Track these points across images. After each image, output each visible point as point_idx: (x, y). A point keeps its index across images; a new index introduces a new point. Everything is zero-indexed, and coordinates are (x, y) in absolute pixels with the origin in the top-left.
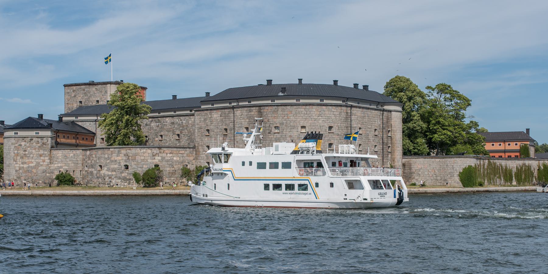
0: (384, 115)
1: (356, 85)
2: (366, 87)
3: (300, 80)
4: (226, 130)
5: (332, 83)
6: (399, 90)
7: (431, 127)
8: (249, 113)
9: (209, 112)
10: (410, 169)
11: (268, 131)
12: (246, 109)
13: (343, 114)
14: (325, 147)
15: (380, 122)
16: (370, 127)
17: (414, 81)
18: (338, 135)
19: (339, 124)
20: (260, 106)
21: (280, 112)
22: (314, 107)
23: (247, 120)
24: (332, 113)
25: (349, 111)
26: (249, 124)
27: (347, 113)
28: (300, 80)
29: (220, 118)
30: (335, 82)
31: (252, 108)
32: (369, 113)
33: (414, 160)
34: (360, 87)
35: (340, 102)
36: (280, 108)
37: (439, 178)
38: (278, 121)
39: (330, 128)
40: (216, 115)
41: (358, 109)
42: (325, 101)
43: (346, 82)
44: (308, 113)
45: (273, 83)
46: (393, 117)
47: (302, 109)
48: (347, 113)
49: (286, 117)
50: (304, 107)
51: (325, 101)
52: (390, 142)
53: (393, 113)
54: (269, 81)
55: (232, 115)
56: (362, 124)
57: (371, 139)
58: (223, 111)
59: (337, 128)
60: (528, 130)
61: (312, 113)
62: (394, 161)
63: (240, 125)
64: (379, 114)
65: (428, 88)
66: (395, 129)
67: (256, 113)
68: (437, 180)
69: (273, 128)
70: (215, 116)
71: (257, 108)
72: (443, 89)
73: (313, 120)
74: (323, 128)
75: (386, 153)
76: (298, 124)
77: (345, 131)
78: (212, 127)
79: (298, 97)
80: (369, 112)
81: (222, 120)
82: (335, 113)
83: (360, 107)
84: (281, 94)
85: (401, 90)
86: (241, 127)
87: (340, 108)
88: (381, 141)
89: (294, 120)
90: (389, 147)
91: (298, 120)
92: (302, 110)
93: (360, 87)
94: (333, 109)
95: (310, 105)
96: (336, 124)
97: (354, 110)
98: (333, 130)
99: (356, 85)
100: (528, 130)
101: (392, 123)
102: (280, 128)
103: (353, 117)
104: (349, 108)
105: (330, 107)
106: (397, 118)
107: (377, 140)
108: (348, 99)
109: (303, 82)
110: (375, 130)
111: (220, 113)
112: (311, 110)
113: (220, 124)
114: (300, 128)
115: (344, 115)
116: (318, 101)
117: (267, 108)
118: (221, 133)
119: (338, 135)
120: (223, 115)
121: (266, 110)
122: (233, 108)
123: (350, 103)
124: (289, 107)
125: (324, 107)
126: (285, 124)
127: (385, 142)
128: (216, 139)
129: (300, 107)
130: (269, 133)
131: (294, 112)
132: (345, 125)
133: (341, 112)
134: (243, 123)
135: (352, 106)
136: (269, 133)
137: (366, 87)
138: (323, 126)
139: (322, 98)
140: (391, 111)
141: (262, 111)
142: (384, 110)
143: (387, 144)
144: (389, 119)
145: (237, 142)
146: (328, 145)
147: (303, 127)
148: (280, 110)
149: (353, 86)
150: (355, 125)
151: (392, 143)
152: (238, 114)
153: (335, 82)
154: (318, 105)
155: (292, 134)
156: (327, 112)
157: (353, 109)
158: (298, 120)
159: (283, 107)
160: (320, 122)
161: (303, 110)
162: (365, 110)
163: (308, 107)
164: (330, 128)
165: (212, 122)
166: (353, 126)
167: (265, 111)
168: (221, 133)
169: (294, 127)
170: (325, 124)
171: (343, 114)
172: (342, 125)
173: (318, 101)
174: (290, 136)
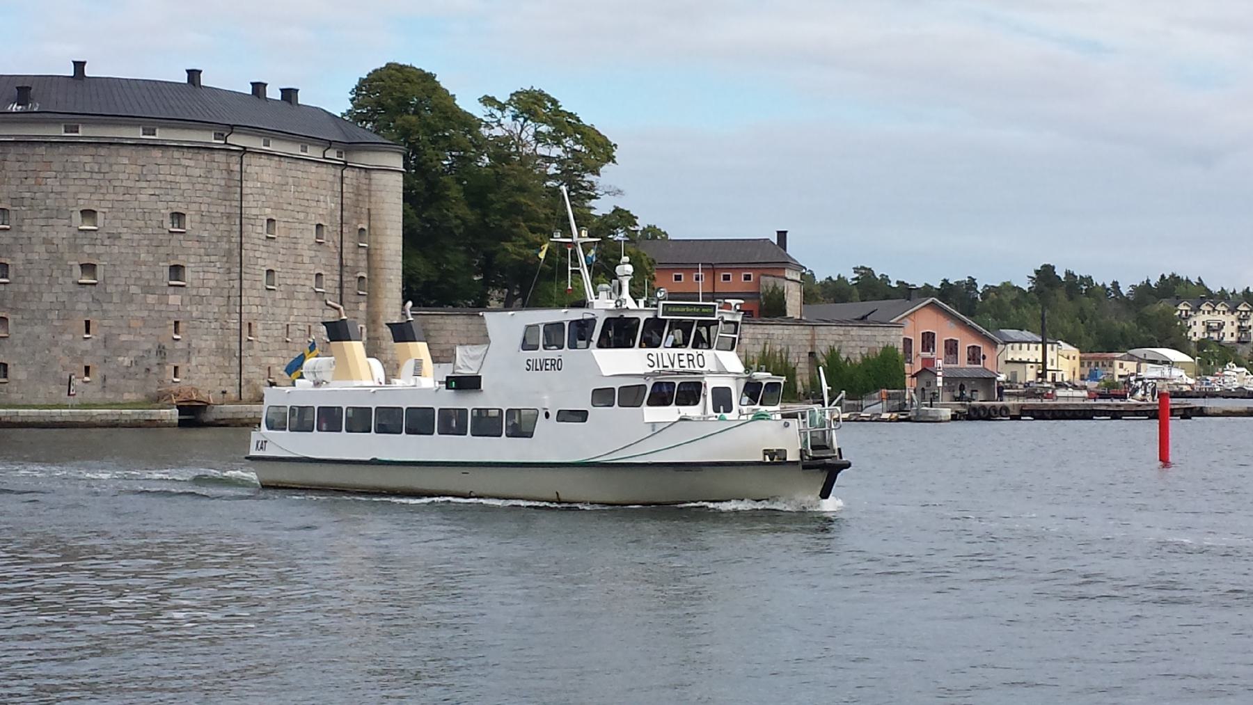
0: (346, 181)
1: (259, 88)
2: (289, 95)
3: (79, 66)
5: (184, 79)
6: (400, 104)
7: (494, 219)
13: (216, 174)
14: (159, 276)
15: (333, 205)
16: (301, 216)
17: (444, 81)
19: (204, 208)
22: (123, 151)
24: (181, 171)
25: (237, 168)
28: (79, 66)
30: (194, 75)
32: (300, 174)
33: (438, 320)
34: (273, 93)
35: (208, 138)
39: (178, 217)
41: (264, 160)
42: (160, 135)
43: (228, 75)
44: (105, 168)
46: (373, 188)
47: (84, 158)
48: (230, 172)
49: (31, 181)
50: (92, 150)
51: (160, 135)
52: (363, 264)
53: (376, 176)
56: (275, 208)
57: (307, 254)
59: (197, 218)
60: (782, 235)
61: (115, 168)
62: (374, 322)
64: (331, 178)
65: (488, 101)
72: (531, 104)
73: (121, 190)
74: (153, 216)
75: (353, 299)
76: (71, 201)
77: (222, 227)
79: (73, 119)
80: (298, 171)
82: (189, 171)
83: (270, 155)
84: (15, 108)
85: (403, 105)
87: (206, 156)
88: (337, 262)
89: (59, 189)
90: (362, 278)
91: (72, 189)
93: (273, 93)
94: (187, 160)
96: (195, 207)
97: (254, 166)
99: (259, 88)
100: (782, 235)
101: (372, 207)
102: (13, 215)
103: (248, 186)
104: (236, 159)
105: (177, 154)
106: (389, 192)
107: (323, 257)
108: (232, 128)
109: (88, 72)
110: (319, 226)
112: (112, 160)
114: (77, 217)
115: (218, 177)
116: (138, 133)
119: (200, 239)
123: (237, 140)
124: (41, 150)
125: (157, 153)
126: (27, 202)
127: (350, 263)
129: (79, 149)
131: (55, 166)
132: (222, 209)
135: (245, 150)
137: (289, 95)
139: (150, 123)
143: (354, 271)
144: (364, 193)
146: (167, 270)
147: (88, 214)
150: (255, 212)
151: (369, 269)
153: (194, 75)
157: (246, 159)
158: (72, 189)
159: (23, 149)
160: (143, 197)
161: (88, 159)
162: (285, 164)
163: (103, 151)
166: (246, 212)
169: (57, 213)
170: (160, 205)
171: (216, 174)
172: (213, 209)
173: (138, 133)
174: (48, 242)
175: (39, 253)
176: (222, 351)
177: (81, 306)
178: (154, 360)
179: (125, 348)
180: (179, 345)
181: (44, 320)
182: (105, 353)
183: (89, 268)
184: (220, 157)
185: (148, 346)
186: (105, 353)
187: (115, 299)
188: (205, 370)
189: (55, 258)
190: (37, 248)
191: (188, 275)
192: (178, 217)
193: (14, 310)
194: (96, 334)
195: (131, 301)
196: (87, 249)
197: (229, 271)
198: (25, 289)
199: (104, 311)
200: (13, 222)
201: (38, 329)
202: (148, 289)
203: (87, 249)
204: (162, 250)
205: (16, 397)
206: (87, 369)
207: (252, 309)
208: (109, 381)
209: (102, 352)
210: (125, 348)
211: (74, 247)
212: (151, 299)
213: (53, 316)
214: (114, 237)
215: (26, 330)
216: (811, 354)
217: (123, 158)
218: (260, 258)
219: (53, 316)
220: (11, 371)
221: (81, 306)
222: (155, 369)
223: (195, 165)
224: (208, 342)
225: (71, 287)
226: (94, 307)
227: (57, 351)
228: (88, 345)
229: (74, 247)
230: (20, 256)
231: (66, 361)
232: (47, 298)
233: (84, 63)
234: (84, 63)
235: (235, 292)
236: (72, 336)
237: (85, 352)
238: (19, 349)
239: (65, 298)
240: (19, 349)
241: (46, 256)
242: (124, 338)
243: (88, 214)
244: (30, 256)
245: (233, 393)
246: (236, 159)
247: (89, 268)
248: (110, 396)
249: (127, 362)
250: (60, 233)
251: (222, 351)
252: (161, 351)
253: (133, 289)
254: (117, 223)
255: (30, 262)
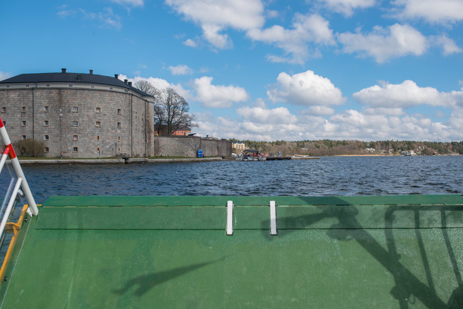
2: (130, 83)
3: (91, 71)
4: (24, 108)
8: (49, 95)
9: (5, 92)
10: (158, 144)
11: (67, 111)
12: (46, 91)
13: (127, 100)
18: (124, 116)
20: (60, 89)
21: (78, 95)
22: (107, 93)
23: (47, 100)
26: (49, 104)
27: (130, 100)
28: (91, 71)
29: (17, 98)
31: (52, 91)
36: (79, 92)
37: (178, 151)
38: (77, 102)
39: (119, 110)
40: (13, 95)
42: (114, 89)
45: (67, 71)
47: (97, 94)
48: (130, 100)
50: (99, 92)
51: (114, 89)
53: (150, 104)
54: (64, 70)
55: (31, 95)
58: (21, 91)
61: (105, 97)
63: (39, 105)
66: (151, 115)
67: (57, 95)
68: (177, 153)
69: (72, 108)
70: (12, 96)
71: (57, 91)
76: (94, 106)
78: (9, 105)
81: (19, 100)
86: (41, 106)
89: (91, 102)
91: (94, 102)
92: (97, 94)
95: (104, 91)
98: (122, 112)
99: (126, 81)
105: (119, 94)
109: (94, 73)
111: (17, 93)
113: (18, 103)
114: (95, 109)
117: (66, 91)
118: (19, 111)
119: (124, 116)
120: (21, 95)
121: (65, 93)
122: (33, 89)
124: (86, 92)
125: (114, 94)
126: (83, 105)
128: (13, 116)
130: (69, 112)
131: (90, 96)
133: (126, 99)
134: (43, 103)
135: (133, 95)
136: (68, 112)
138: (114, 109)
140: (148, 102)
141: (62, 93)
142: (146, 101)
144: (148, 107)
145: (37, 119)
147: (98, 108)
148: (78, 93)
149: (124, 81)
152: (37, 95)
154: (110, 91)
155: (89, 114)
156: (116, 98)
157: (133, 97)
158: (94, 102)
159: (81, 91)
160: (112, 105)
161: (98, 95)
163: (102, 93)
164: (119, 110)
165: (8, 101)
167: (65, 93)
168: (19, 111)
169: (90, 108)
170: (115, 107)
171: (127, 100)
173: (108, 88)
174: (88, 116)
175: (86, 118)
176: (128, 145)
177: (97, 133)
178: (114, 147)
179: (108, 144)
180: (120, 143)
181: (87, 136)
182: (102, 145)
183: (98, 123)
184: (128, 96)
185: (113, 143)
186: (102, 145)
187: (105, 131)
188: (125, 149)
189: (90, 120)
190: (85, 117)
191: (122, 125)
192: (119, 110)
193: (79, 133)
194: (100, 140)
195: (109, 132)
196: (98, 118)
197: (129, 125)
198: (82, 128)
199: (102, 134)
200: (79, 110)
201: (86, 139)
202: (113, 129)
203: (98, 118)
204: (116, 119)
205: (80, 156)
206: (98, 149)
207: (134, 134)
208: (104, 152)
209: (102, 145)
210: (108, 144)
211: (95, 117)
212: (113, 131)
213: (89, 135)
214: (105, 115)
215: (83, 139)
216: (218, 147)
217: (107, 94)
218: (135, 122)
219: (89, 135)
220: (79, 149)
221: (97, 133)
222: (114, 149)
223: (123, 97)
224: (125, 142)
225: (94, 128)
226: (100, 133)
227: (91, 144)
228: (98, 143)
229: (95, 117)
230: (81, 119)
231: (93, 147)
232: (88, 130)
233: (92, 71)
234: (92, 71)
235: (131, 130)
236: (94, 140)
237: (98, 145)
238: (81, 144)
239: (92, 130)
240: (81, 144)
241: (88, 119)
242: (107, 141)
243: (98, 108)
244: (84, 119)
245: (131, 156)
246: (131, 97)
247: (98, 123)
248: (104, 156)
249: (108, 147)
250: (91, 113)
251: (128, 145)
252: (116, 144)
253: (109, 129)
254: (105, 111)
255: (83, 121)
